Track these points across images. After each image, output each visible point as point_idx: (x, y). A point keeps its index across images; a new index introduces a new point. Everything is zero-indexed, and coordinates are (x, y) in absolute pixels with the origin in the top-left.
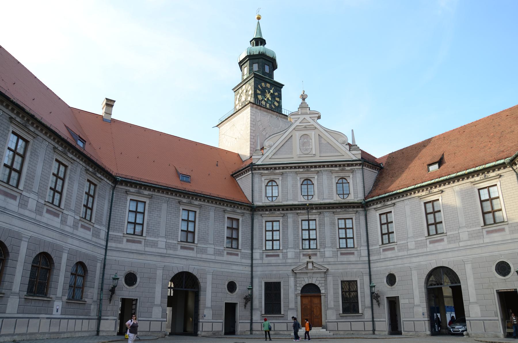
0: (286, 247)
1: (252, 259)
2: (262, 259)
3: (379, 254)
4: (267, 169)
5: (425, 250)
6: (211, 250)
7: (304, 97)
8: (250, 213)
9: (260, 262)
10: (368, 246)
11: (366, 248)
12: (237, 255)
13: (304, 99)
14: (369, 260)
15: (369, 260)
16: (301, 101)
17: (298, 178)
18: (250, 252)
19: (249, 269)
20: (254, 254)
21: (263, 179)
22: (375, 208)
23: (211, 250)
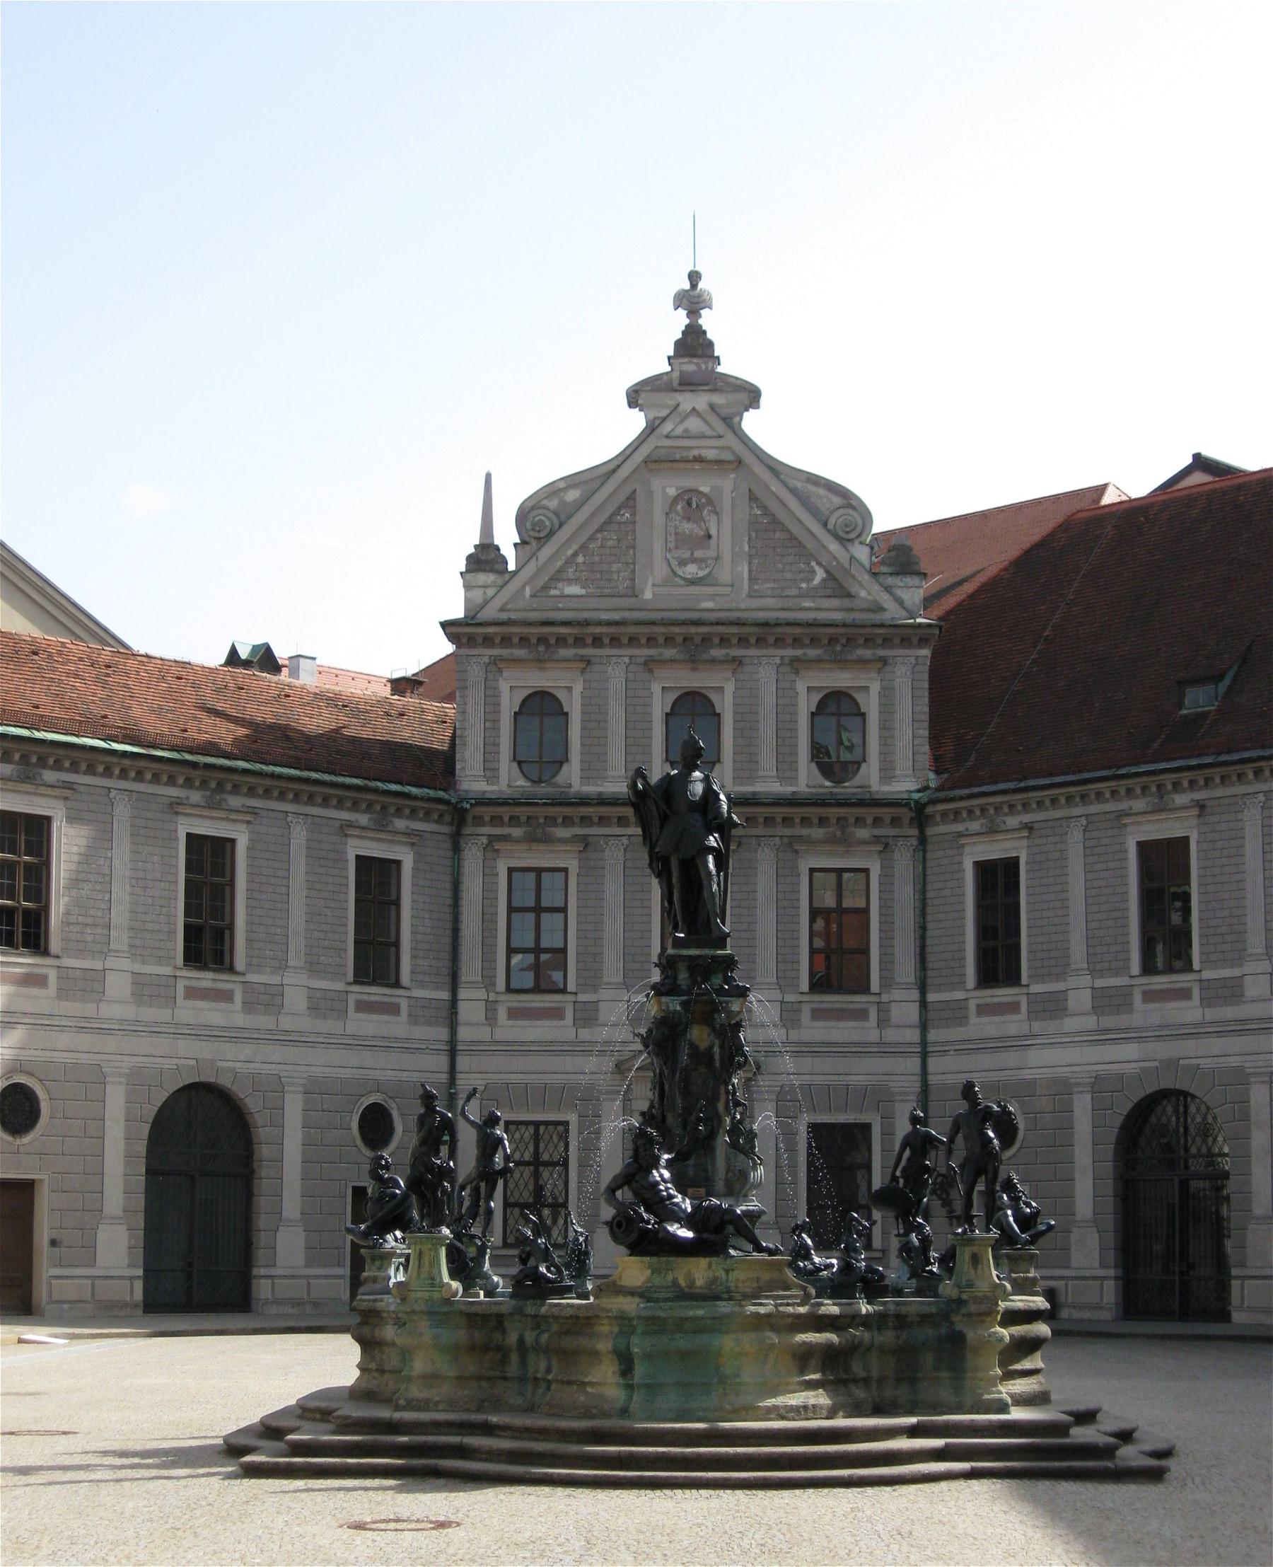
0: (592, 980)
1: (453, 1024)
2: (491, 1018)
3: (963, 1020)
4: (524, 641)
5: (1123, 1020)
6: (296, 999)
7: (692, 300)
8: (445, 829)
9: (484, 1033)
10: (923, 987)
11: (915, 995)
12: (393, 1009)
13: (694, 313)
14: (924, 1043)
15: (924, 1043)
16: (681, 320)
17: (656, 689)
18: (445, 995)
19: (443, 1062)
20: (462, 1006)
21: (504, 686)
22: (960, 835)
23: (296, 999)
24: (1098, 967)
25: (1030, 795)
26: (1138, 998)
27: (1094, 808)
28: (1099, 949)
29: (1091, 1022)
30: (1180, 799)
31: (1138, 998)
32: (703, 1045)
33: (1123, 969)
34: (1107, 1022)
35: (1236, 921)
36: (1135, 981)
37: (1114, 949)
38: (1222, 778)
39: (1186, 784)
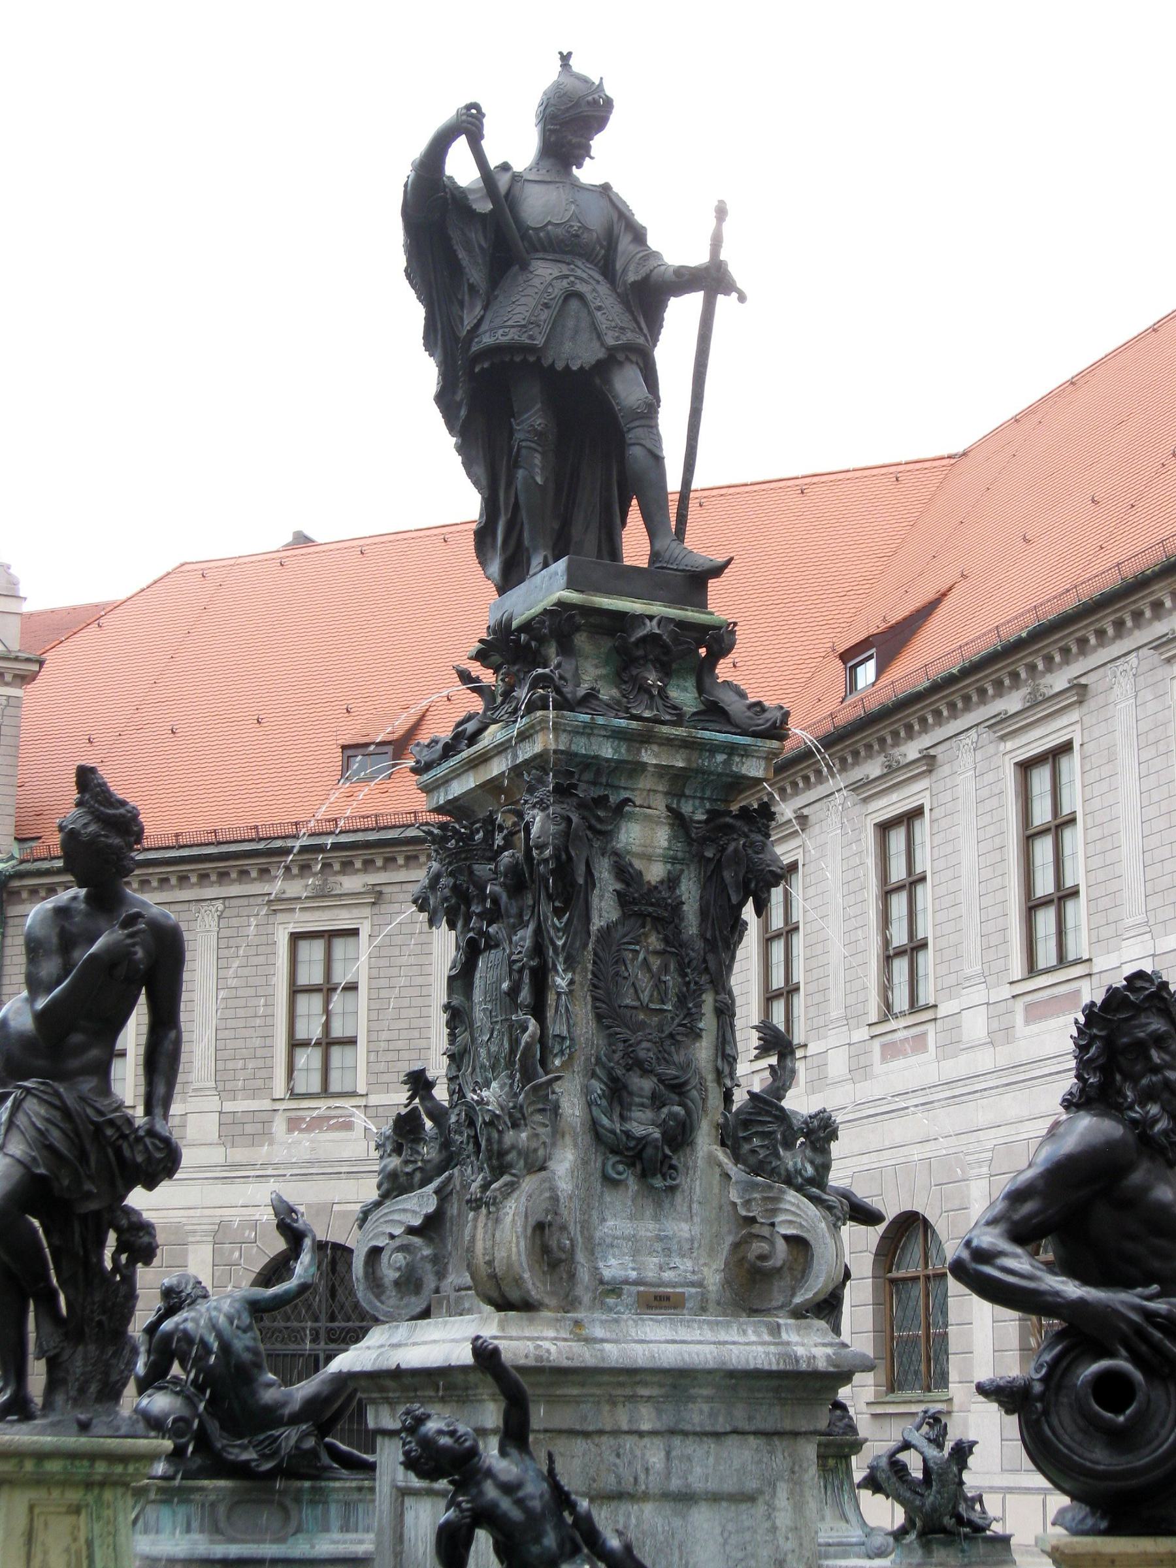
24: (229, 1086)
25: (151, 870)
26: (279, 1125)
27: (235, 890)
28: (230, 1065)
29: (217, 1155)
30: (351, 883)
31: (279, 1125)
32: (655, 872)
33: (262, 1090)
34: (239, 1155)
35: (416, 1034)
36: (277, 1106)
37: (251, 1064)
38: (408, 859)
39: (358, 864)
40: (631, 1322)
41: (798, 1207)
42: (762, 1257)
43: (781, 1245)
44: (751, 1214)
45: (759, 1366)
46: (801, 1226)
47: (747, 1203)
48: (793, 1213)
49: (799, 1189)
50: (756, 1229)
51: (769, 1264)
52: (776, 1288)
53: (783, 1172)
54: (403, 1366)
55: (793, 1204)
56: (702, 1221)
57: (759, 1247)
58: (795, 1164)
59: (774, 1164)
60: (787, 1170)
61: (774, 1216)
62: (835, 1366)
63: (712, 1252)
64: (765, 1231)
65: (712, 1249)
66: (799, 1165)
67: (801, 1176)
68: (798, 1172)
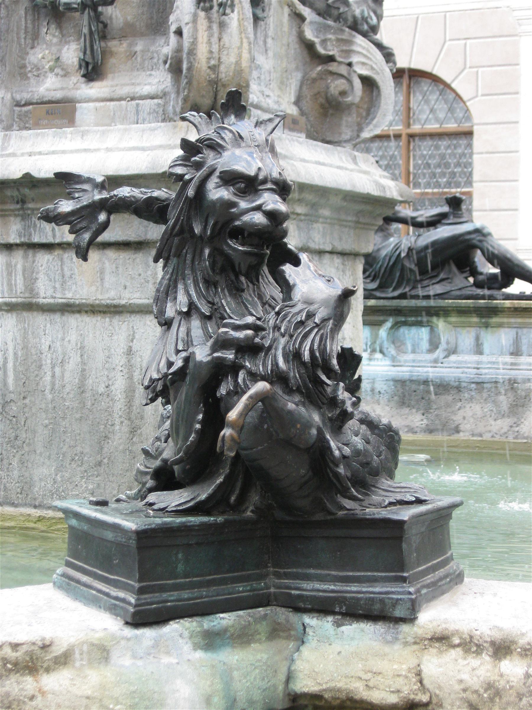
40: (287, 141)
41: (368, 51)
42: (343, 93)
43: (357, 83)
44: (331, 53)
45: (370, 192)
46: (372, 68)
47: (324, 42)
48: (365, 56)
49: (365, 35)
50: (333, 67)
51: (349, 99)
52: (344, 123)
53: (350, 19)
54: (36, 174)
55: (364, 48)
56: (274, 55)
57: (336, 86)
58: (363, 11)
59: (341, 10)
60: (354, 17)
61: (348, 57)
62: (402, 196)
63: (283, 84)
64: (343, 70)
65: (282, 83)
66: (366, 14)
67: (367, 23)
68: (365, 20)
